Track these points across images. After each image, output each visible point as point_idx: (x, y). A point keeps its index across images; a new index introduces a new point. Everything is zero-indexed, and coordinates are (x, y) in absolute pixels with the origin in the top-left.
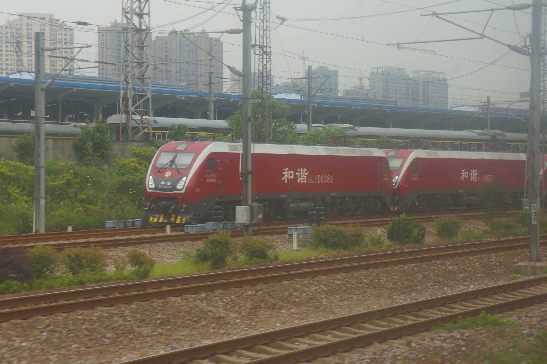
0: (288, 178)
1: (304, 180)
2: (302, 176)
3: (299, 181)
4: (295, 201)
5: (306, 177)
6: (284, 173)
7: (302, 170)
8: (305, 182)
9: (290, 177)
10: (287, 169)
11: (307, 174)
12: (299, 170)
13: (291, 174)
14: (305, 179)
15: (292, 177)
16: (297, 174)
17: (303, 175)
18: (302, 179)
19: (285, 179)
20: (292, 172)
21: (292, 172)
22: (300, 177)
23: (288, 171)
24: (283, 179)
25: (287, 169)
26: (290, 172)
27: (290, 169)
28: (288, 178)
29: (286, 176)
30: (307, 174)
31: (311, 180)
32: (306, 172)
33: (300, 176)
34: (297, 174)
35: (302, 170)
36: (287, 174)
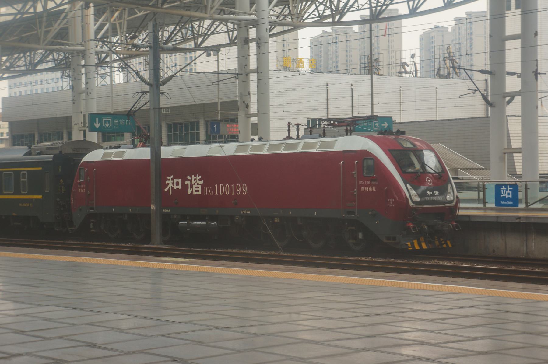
0: (173, 188)
1: (198, 191)
2: (194, 186)
3: (189, 192)
4: (184, 218)
5: (200, 186)
6: (167, 182)
7: (194, 177)
8: (199, 193)
9: (176, 187)
10: (172, 177)
11: (201, 182)
12: (189, 177)
13: (177, 184)
14: (200, 189)
15: (179, 187)
16: (186, 182)
17: (196, 185)
22: (192, 186)
23: (172, 179)
24: (166, 190)
25: (172, 177)
26: (175, 180)
27: (176, 177)
28: (173, 188)
29: (170, 185)
30: (201, 182)
31: (208, 191)
32: (200, 180)
33: (192, 186)
34: (186, 182)
35: (194, 177)
36: (172, 184)
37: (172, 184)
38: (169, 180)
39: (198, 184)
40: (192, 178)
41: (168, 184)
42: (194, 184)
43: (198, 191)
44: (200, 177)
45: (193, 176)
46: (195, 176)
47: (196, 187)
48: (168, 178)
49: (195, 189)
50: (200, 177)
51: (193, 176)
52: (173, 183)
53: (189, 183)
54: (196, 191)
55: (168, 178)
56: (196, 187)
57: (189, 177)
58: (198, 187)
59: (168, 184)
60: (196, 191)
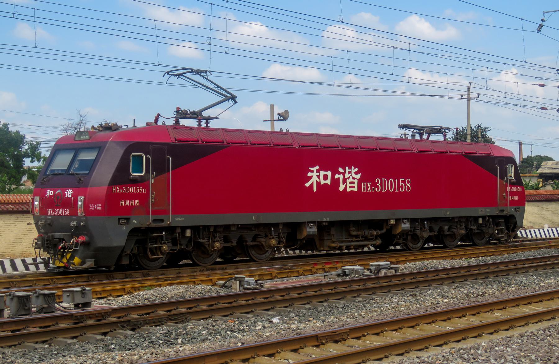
0: (318, 183)
1: (354, 187)
2: (348, 181)
3: (342, 188)
5: (356, 181)
6: (309, 174)
7: (347, 170)
8: (356, 189)
9: (323, 182)
10: (317, 167)
11: (358, 176)
12: (341, 170)
13: (325, 177)
14: (356, 185)
15: (328, 182)
16: (337, 176)
17: (350, 179)
19: (312, 185)
20: (329, 173)
21: (329, 173)
23: (318, 171)
24: (307, 185)
25: (317, 167)
26: (322, 173)
28: (318, 183)
29: (314, 179)
30: (358, 176)
31: (367, 187)
32: (356, 173)
33: (345, 181)
34: (337, 176)
35: (347, 170)
36: (316, 177)
37: (316, 177)
38: (312, 171)
39: (354, 178)
40: (345, 170)
41: (311, 177)
42: (349, 178)
43: (354, 187)
44: (356, 169)
45: (347, 168)
46: (350, 168)
47: (350, 183)
49: (348, 185)
50: (356, 169)
51: (347, 168)
52: (319, 177)
53: (341, 176)
54: (350, 187)
56: (350, 183)
57: (341, 170)
58: (354, 183)
59: (311, 177)
60: (350, 187)
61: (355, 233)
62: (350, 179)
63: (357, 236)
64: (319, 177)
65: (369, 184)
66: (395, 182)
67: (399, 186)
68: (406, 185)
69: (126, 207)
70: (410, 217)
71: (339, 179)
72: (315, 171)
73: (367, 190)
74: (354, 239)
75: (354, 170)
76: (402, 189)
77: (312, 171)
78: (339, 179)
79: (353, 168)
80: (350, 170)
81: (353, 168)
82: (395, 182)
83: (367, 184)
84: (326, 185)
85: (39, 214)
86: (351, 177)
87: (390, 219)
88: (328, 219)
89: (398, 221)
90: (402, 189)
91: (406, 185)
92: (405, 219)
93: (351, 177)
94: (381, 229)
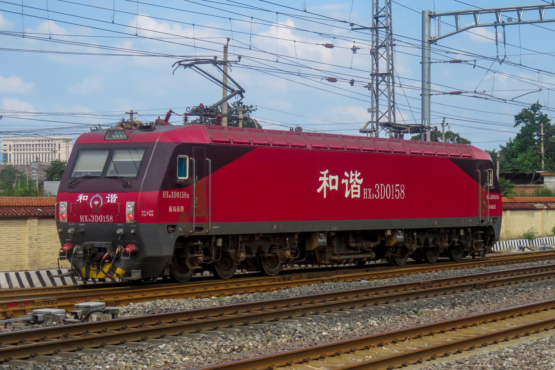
0: (328, 189)
1: (356, 193)
2: (352, 186)
3: (347, 195)
5: (359, 187)
6: (321, 179)
8: (358, 196)
9: (332, 188)
10: (327, 171)
12: (346, 174)
14: (358, 191)
15: (336, 187)
16: (343, 181)
17: (354, 184)
18: (353, 191)
20: (336, 178)
21: (336, 178)
22: (349, 187)
23: (328, 176)
24: (319, 190)
25: (327, 171)
26: (331, 177)
27: (331, 173)
28: (328, 189)
29: (325, 184)
30: (360, 181)
31: (368, 194)
32: (359, 178)
33: (350, 185)
34: (343, 181)
35: (352, 175)
37: (327, 182)
38: (323, 176)
39: (357, 184)
40: (349, 174)
41: (322, 181)
42: (353, 183)
43: (356, 193)
44: (359, 174)
45: (351, 172)
46: (354, 173)
48: (321, 173)
49: (353, 191)
51: (351, 172)
52: (328, 181)
55: (321, 173)
57: (346, 174)
59: (322, 181)
61: (353, 245)
62: (354, 184)
63: (355, 249)
64: (328, 181)
65: (370, 190)
66: (391, 187)
67: (395, 193)
68: (400, 191)
69: (173, 213)
70: (404, 228)
71: (345, 184)
72: (325, 175)
73: (368, 197)
74: (352, 252)
75: (358, 174)
76: (397, 197)
77: (323, 176)
78: (345, 184)
79: (356, 171)
80: (354, 175)
81: (356, 171)
82: (391, 187)
83: (368, 190)
84: (334, 190)
85: (66, 221)
86: (355, 183)
87: (387, 230)
88: (336, 229)
89: (393, 231)
90: (397, 197)
91: (400, 191)
92: (399, 230)
93: (355, 183)
94: (376, 241)
